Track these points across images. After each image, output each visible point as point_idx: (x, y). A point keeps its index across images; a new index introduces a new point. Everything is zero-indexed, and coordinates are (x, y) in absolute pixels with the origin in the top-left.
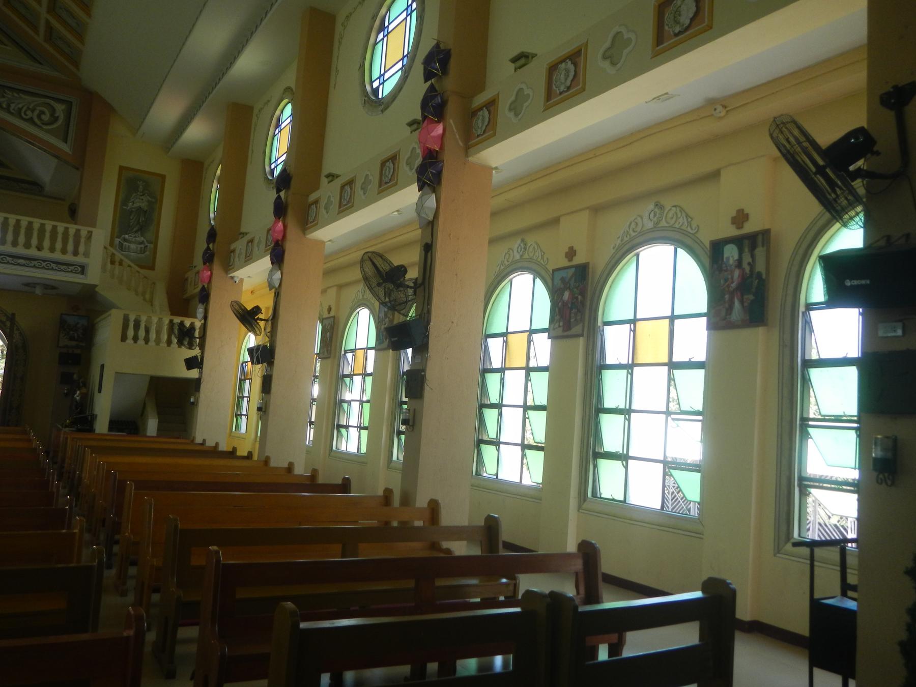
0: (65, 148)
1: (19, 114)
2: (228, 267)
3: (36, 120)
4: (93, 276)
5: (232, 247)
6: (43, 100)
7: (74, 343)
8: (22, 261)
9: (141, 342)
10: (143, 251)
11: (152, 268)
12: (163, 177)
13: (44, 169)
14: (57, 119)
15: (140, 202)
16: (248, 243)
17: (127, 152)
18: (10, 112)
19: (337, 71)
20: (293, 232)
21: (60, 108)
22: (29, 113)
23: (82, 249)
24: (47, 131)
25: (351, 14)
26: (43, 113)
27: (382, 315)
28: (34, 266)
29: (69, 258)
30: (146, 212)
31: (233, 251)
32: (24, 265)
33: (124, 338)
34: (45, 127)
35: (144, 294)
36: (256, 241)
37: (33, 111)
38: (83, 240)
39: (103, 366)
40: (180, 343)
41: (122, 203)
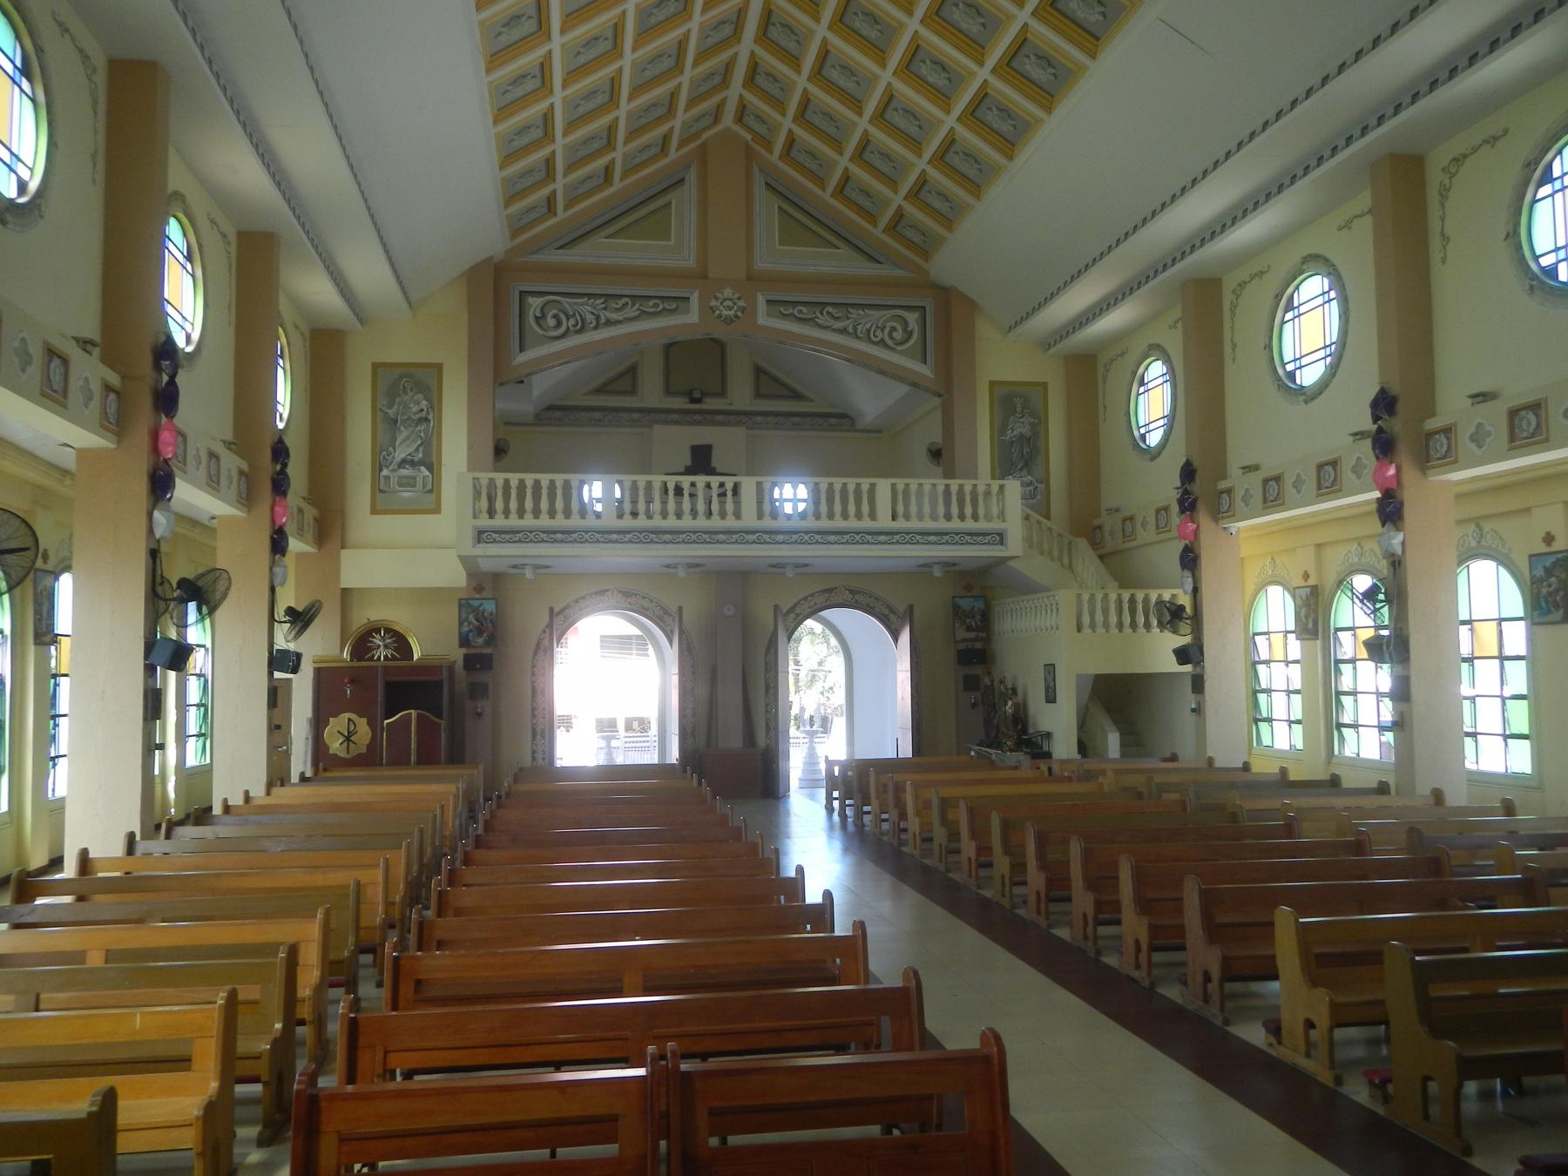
0: (925, 371)
2: (1217, 514)
4: (1015, 545)
5: (1223, 485)
7: (973, 635)
8: (932, 538)
9: (1100, 630)
10: (1032, 496)
11: (1048, 517)
12: (1045, 385)
13: (870, 399)
14: (910, 334)
15: (1020, 428)
16: (1266, 481)
17: (1001, 360)
18: (858, 338)
19: (1445, 238)
20: (1410, 475)
21: (912, 318)
22: (879, 333)
23: (995, 511)
24: (901, 353)
25: (1465, 156)
26: (893, 329)
27: (1540, 572)
28: (947, 543)
29: (982, 525)
30: (1028, 440)
31: (1229, 491)
33: (1079, 630)
35: (1060, 559)
36: (1288, 481)
38: (981, 499)
39: (1050, 669)
40: (1161, 625)
41: (999, 430)
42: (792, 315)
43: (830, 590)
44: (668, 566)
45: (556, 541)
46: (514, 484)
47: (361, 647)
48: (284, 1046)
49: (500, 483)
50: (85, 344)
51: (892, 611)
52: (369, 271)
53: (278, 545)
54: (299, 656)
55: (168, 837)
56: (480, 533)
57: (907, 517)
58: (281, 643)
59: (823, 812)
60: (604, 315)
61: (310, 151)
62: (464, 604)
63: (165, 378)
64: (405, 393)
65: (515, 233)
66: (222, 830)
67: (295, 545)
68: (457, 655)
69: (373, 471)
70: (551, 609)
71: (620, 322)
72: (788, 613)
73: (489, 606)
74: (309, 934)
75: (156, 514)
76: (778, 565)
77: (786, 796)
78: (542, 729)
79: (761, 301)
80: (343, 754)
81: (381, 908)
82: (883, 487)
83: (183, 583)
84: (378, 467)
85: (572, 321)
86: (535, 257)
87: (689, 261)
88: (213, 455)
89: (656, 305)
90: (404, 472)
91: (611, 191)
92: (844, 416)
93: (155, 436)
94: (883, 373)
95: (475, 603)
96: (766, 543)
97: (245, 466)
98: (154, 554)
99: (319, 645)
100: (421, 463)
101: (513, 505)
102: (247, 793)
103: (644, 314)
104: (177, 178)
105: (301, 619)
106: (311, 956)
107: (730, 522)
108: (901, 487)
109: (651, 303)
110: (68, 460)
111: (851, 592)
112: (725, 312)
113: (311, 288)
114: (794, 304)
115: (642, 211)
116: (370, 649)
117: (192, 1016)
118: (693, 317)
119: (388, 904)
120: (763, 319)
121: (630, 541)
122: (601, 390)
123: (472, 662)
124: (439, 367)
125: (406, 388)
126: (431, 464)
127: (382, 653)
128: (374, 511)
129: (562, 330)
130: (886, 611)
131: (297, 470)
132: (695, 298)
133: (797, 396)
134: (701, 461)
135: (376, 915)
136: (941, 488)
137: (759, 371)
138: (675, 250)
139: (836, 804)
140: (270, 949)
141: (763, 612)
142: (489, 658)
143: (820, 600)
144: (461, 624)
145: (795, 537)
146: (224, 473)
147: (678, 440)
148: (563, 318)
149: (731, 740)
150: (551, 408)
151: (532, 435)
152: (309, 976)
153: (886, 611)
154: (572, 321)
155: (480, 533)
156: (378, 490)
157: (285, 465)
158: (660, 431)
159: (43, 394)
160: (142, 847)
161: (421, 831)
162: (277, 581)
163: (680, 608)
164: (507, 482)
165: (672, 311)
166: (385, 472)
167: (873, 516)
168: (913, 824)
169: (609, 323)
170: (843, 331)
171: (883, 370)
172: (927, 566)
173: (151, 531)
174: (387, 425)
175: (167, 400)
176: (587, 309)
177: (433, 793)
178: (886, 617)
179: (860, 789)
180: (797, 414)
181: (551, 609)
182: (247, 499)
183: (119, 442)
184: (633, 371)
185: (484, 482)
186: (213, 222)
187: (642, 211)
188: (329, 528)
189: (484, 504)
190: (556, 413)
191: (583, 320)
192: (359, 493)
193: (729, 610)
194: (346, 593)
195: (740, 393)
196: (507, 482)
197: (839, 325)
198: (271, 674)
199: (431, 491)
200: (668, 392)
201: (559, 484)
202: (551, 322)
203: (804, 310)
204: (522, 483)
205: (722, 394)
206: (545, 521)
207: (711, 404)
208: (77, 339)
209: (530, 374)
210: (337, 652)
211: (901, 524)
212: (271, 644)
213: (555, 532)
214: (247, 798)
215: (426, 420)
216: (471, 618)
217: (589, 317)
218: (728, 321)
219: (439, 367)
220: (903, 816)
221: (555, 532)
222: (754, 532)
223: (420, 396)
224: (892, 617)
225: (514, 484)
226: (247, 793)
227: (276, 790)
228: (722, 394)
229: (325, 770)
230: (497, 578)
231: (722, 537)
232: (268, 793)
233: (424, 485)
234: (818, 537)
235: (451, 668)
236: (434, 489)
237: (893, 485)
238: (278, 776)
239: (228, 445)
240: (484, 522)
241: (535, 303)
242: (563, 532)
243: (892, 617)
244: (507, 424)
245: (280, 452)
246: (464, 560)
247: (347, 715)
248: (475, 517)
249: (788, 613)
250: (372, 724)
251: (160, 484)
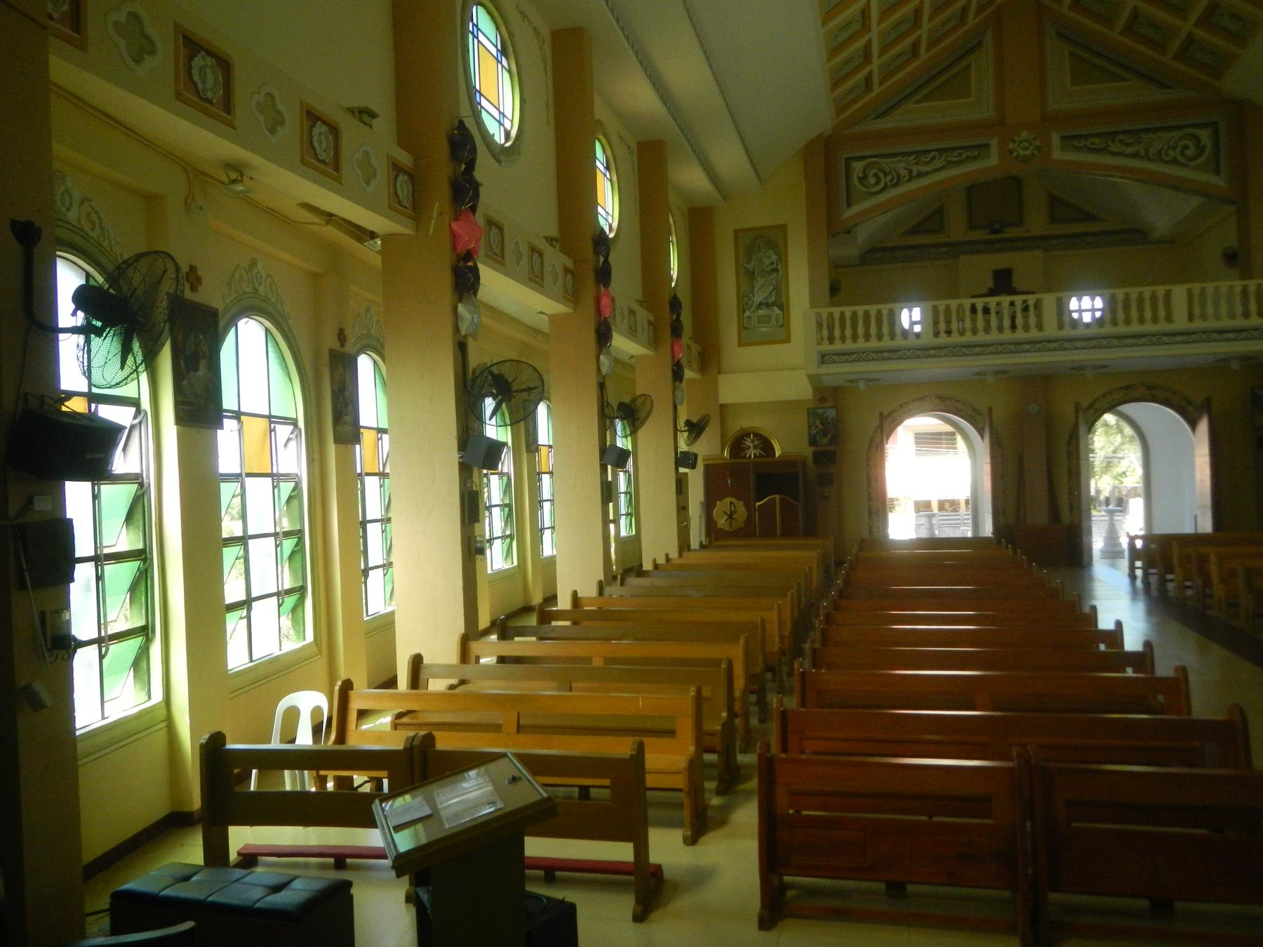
0: (1218, 181)
1: (1159, 158)
3: (1182, 160)
6: (1177, 134)
13: (1161, 213)
14: (1201, 150)
18: (1149, 159)
21: (1205, 135)
22: (1171, 153)
26: (1186, 147)
32: (1233, 340)
34: (1193, 163)
37: (1174, 148)
42: (1085, 146)
43: (1127, 387)
44: (979, 374)
45: (884, 359)
46: (848, 315)
47: (737, 447)
48: (728, 726)
49: (837, 316)
50: (551, 240)
52: (730, 158)
53: (677, 375)
54: (696, 456)
55: (622, 584)
56: (823, 356)
57: (1204, 317)
58: (683, 447)
59: (1126, 580)
60: (915, 169)
61: (687, 72)
62: (811, 413)
63: (602, 259)
64: (759, 250)
65: (840, 110)
66: (658, 581)
67: (688, 374)
68: (808, 452)
69: (738, 315)
70: (881, 414)
71: (927, 173)
73: (831, 413)
74: (736, 652)
75: (602, 357)
76: (1078, 368)
78: (878, 506)
79: (1055, 139)
80: (727, 528)
81: (777, 640)
82: (1179, 293)
83: (622, 406)
84: (742, 309)
85: (889, 178)
86: (858, 129)
87: (988, 112)
88: (632, 312)
89: (960, 155)
90: (761, 312)
91: (917, 63)
92: (1133, 231)
93: (598, 301)
94: (1176, 188)
95: (820, 411)
96: (1066, 349)
97: (652, 319)
98: (602, 386)
99: (707, 447)
100: (775, 304)
101: (848, 332)
102: (667, 555)
103: (950, 164)
104: (600, 111)
105: (696, 429)
106: (739, 670)
107: (1034, 334)
108: (1197, 291)
109: (956, 153)
110: (543, 324)
112: (1022, 153)
113: (689, 178)
114: (1086, 137)
115: (944, 77)
116: (744, 449)
117: (675, 703)
118: (993, 160)
119: (782, 637)
120: (1057, 154)
121: (946, 355)
122: (914, 231)
123: (819, 457)
124: (783, 227)
125: (762, 246)
126: (783, 306)
127: (752, 453)
128: (741, 344)
129: (882, 185)
131: (686, 318)
132: (994, 143)
133: (1090, 217)
134: (1003, 283)
135: (775, 645)
136: (1238, 289)
137: (1053, 200)
138: (975, 105)
139: (1139, 573)
140: (717, 662)
142: (834, 452)
144: (810, 428)
145: (1094, 343)
146: (639, 324)
147: (981, 267)
148: (881, 175)
149: (1038, 516)
150: (873, 250)
151: (858, 277)
152: (739, 684)
154: (889, 178)
155: (823, 356)
156: (743, 328)
157: (679, 315)
158: (964, 259)
159: (530, 279)
160: (607, 590)
161: (799, 584)
162: (678, 401)
163: (990, 409)
164: (842, 314)
165: (975, 158)
166: (747, 314)
167: (1169, 319)
168: (1219, 590)
169: (920, 175)
170: (1135, 155)
171: (1177, 186)
172: (1223, 363)
173: (599, 370)
174: (748, 276)
175: (604, 275)
176: (901, 166)
177: (800, 557)
179: (1162, 560)
180: (1092, 235)
181: (881, 414)
182: (654, 342)
183: (575, 308)
184: (939, 213)
185: (825, 315)
186: (621, 138)
187: (944, 77)
188: (709, 359)
189: (825, 333)
190: (877, 254)
191: (898, 176)
192: (729, 330)
194: (723, 407)
195: (1037, 222)
196: (842, 314)
197: (1130, 150)
198: (677, 470)
199: (782, 326)
200: (972, 226)
201: (885, 312)
202: (872, 180)
203: (1097, 141)
204: (854, 314)
205: (1020, 222)
206: (874, 344)
207: (1010, 233)
208: (546, 238)
209: (856, 225)
210: (719, 452)
211: (1198, 324)
212: (676, 447)
213: (882, 352)
214: (668, 559)
215: (776, 270)
216: (818, 423)
217: (903, 172)
218: (1025, 160)
219: (783, 227)
220: (1207, 583)
221: (882, 352)
222: (1055, 341)
223: (771, 252)
224: (1190, 409)
225: (848, 315)
226: (667, 555)
227: (685, 554)
228: (1020, 222)
229: (716, 540)
230: (837, 391)
231: (1026, 347)
232: (680, 556)
233: (777, 321)
234: (1115, 341)
235: (804, 463)
236: (784, 325)
237: (1189, 290)
238: (684, 545)
239: (640, 303)
240: (826, 347)
241: (858, 166)
242: (889, 351)
243: (1190, 409)
244: (837, 266)
245: (675, 305)
246: (813, 379)
247: (728, 500)
248: (819, 343)
250: (747, 506)
251: (603, 336)
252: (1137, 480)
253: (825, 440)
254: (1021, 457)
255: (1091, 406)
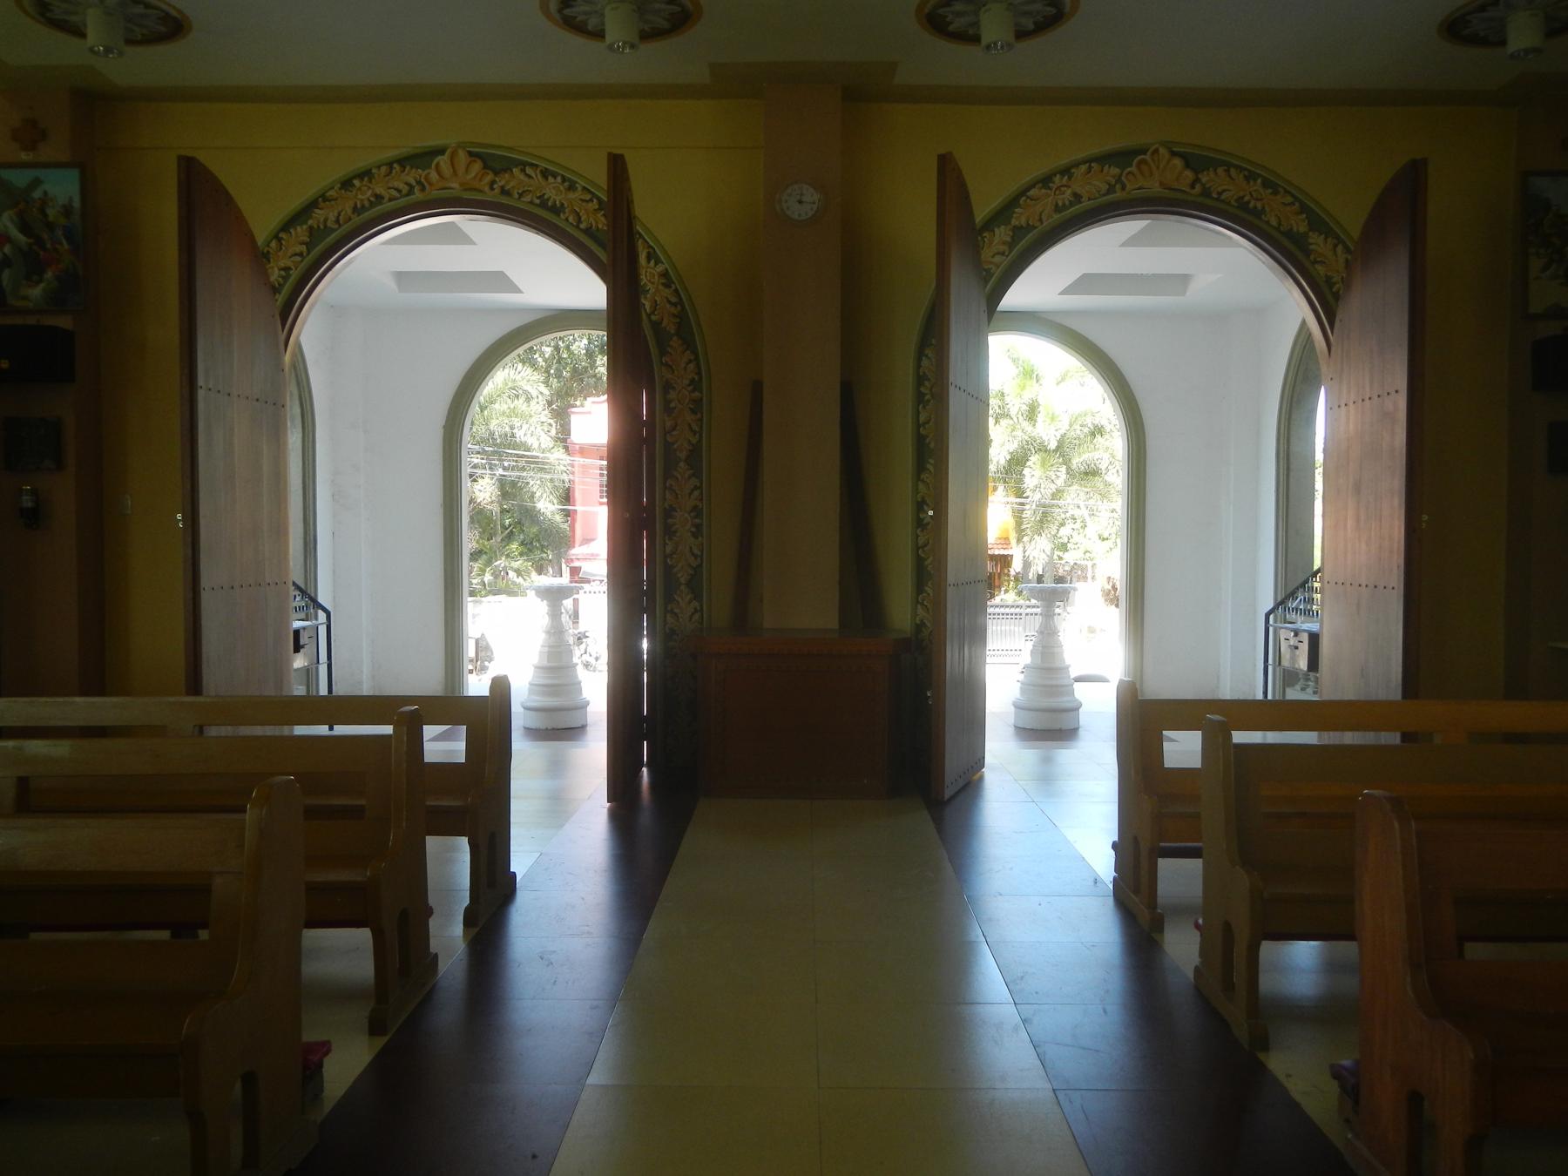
43: (1122, 157)
51: (1318, 223)
72: (989, 224)
73: (62, 188)
77: (970, 785)
95: (19, 178)
111: (1189, 161)
130: (1300, 225)
141: (909, 216)
143: (1091, 186)
153: (1300, 225)
178: (1300, 241)
193: (802, 202)
224: (1317, 242)
243: (1317, 242)
249: (989, 224)
252: (1137, 492)
253: (36, 292)
254: (757, 390)
255: (1002, 214)
